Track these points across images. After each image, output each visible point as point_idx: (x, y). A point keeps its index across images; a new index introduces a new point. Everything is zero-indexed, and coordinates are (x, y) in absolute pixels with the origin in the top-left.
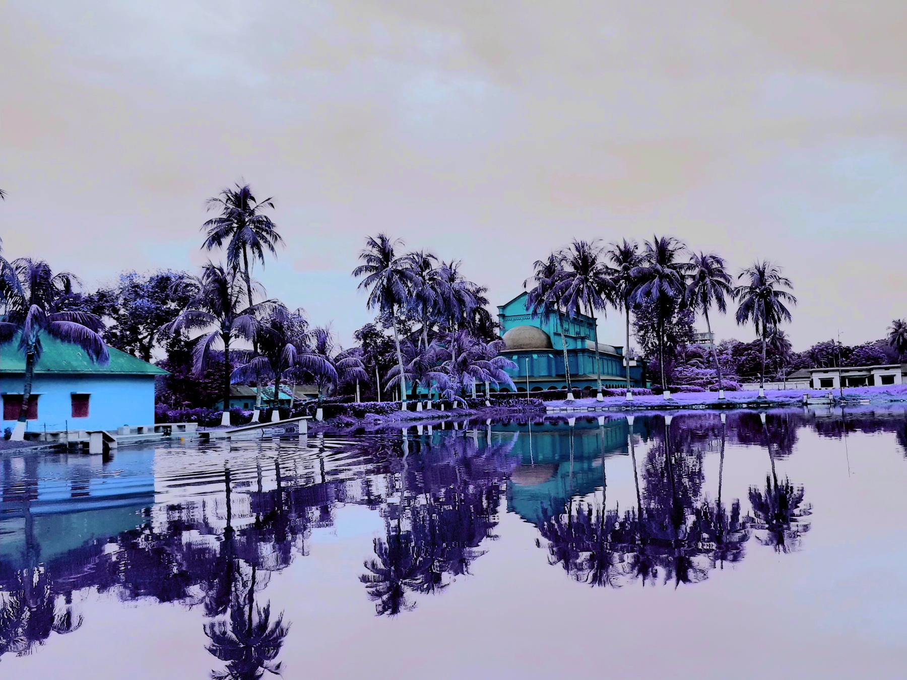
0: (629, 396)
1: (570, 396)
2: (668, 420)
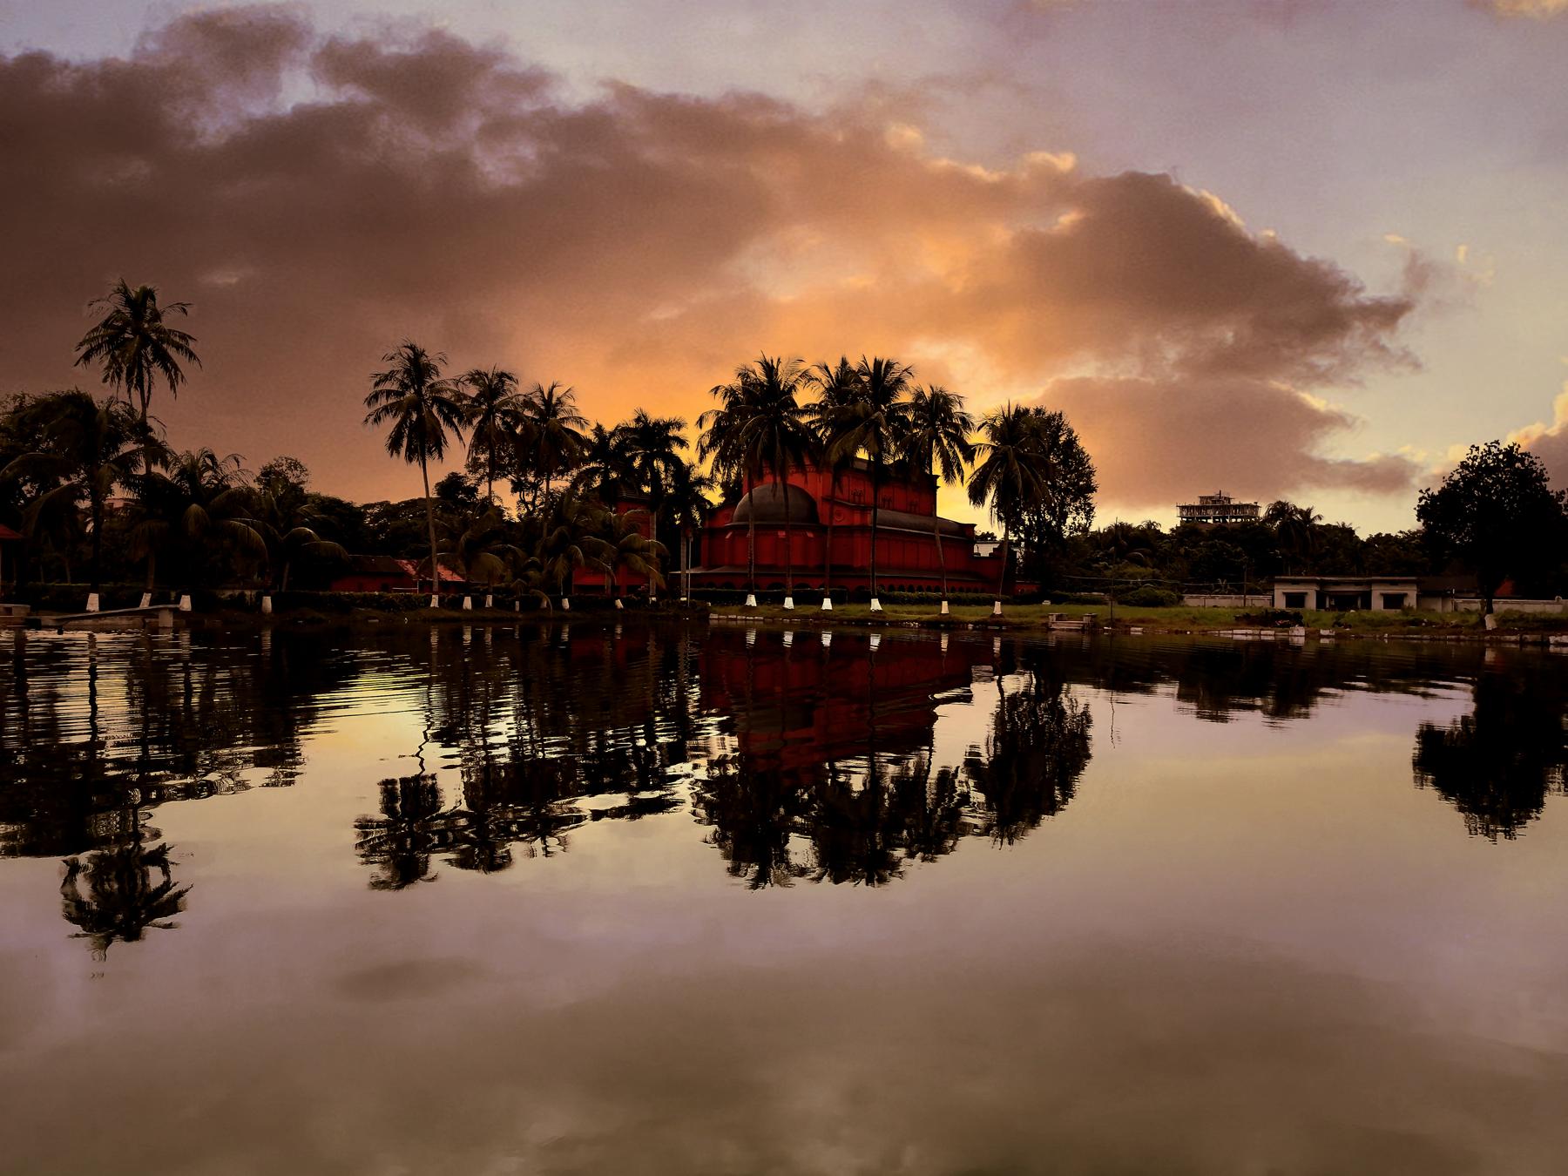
2: (875, 642)
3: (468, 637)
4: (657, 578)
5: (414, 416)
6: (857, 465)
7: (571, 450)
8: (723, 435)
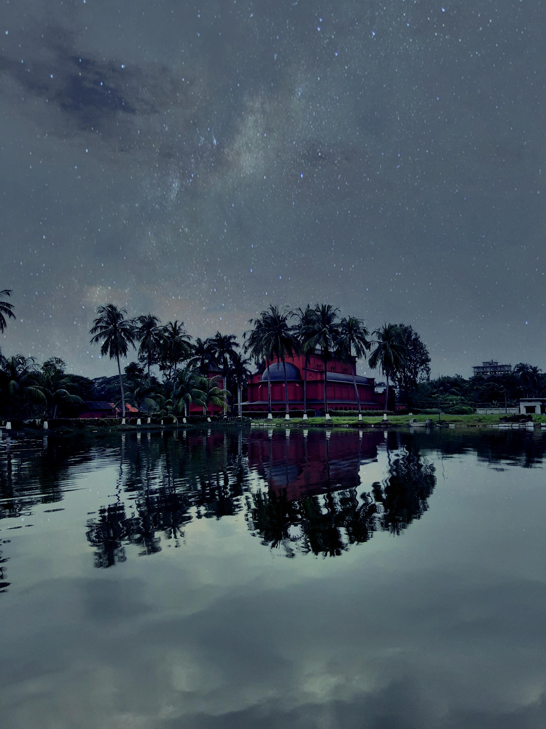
0: (360, 417)
1: (270, 416)
2: (328, 434)
3: (139, 437)
4: (226, 407)
5: (113, 337)
6: (316, 352)
7: (186, 350)
8: (255, 340)
